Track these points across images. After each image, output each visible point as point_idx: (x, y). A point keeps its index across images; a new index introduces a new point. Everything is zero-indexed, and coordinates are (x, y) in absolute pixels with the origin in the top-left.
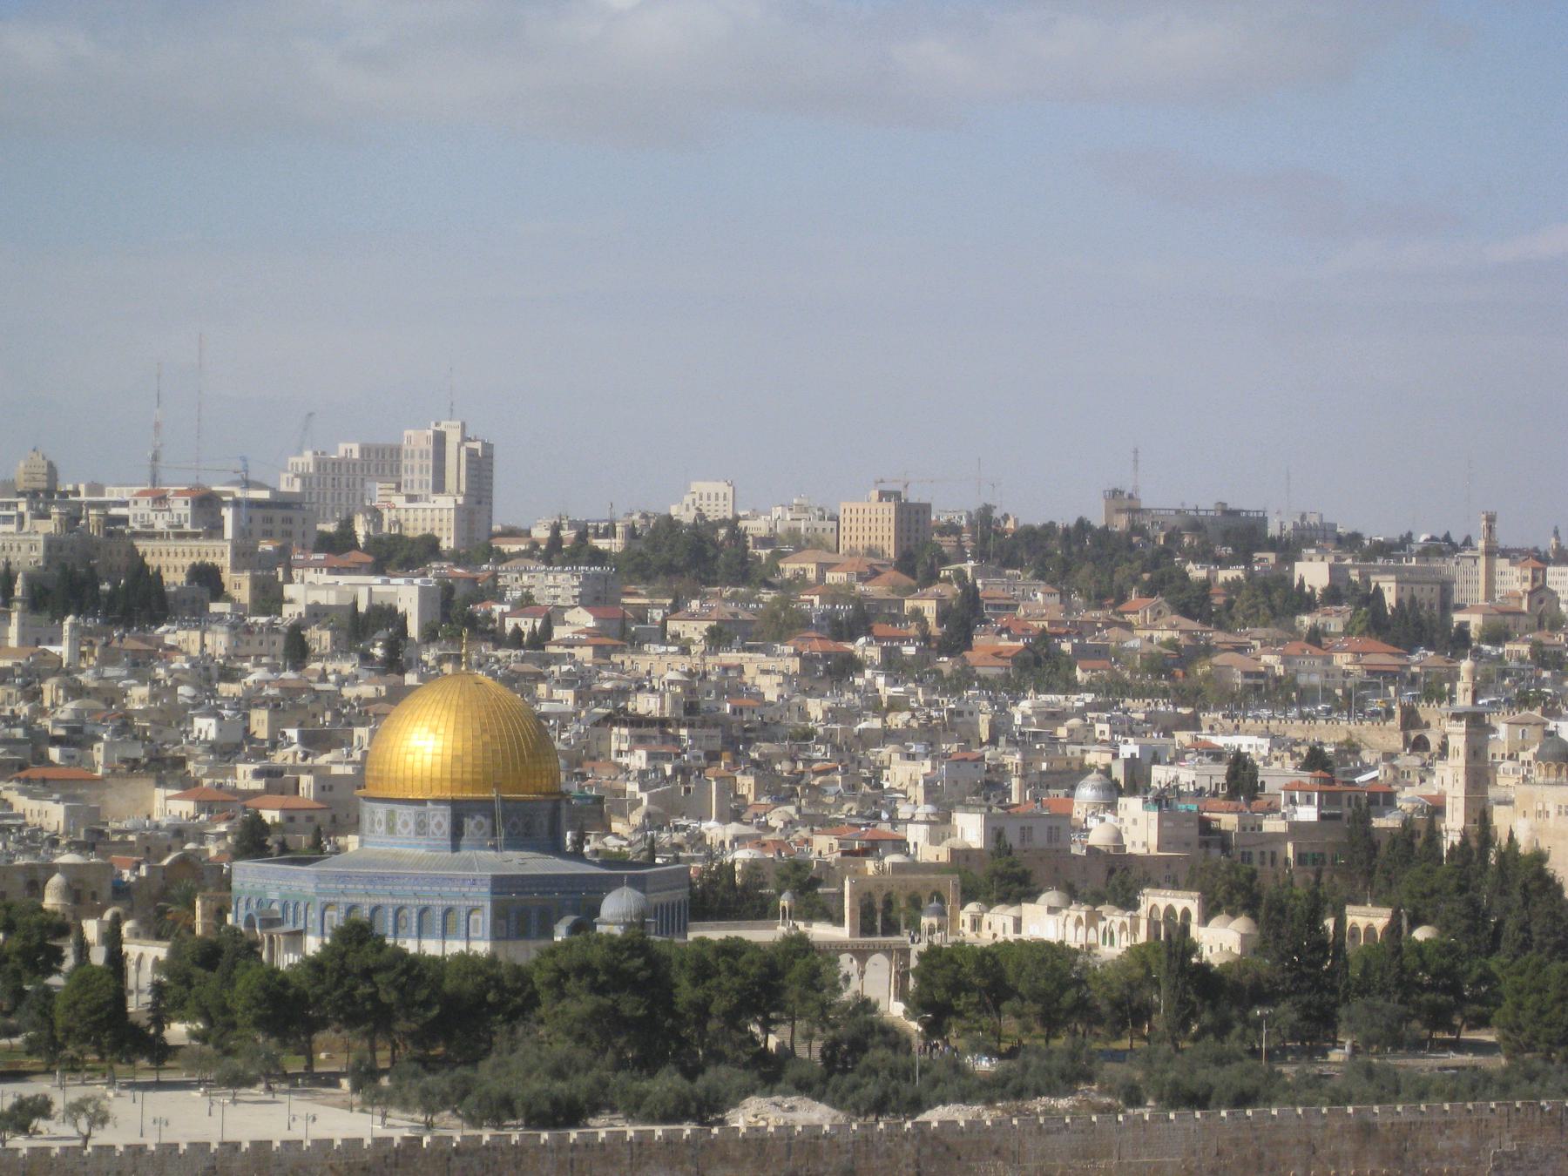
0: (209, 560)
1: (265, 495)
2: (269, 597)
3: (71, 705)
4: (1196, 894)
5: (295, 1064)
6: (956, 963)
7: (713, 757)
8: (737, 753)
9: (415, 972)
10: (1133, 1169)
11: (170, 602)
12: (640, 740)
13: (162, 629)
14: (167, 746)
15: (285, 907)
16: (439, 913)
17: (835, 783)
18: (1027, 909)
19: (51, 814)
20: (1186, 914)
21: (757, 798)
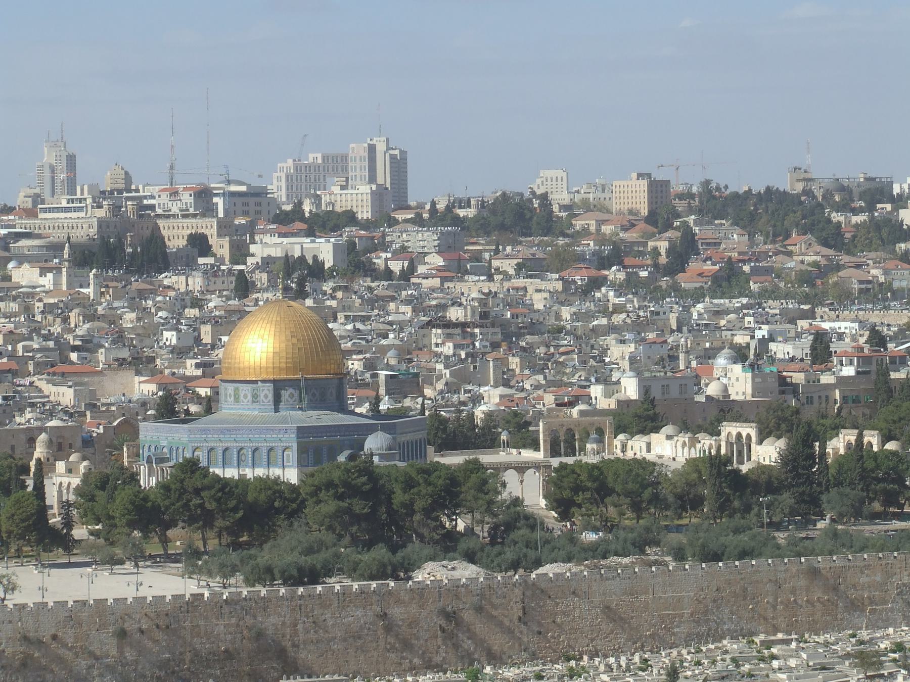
0: (200, 231)
1: (243, 188)
2: (240, 253)
3: (87, 326)
4: (754, 425)
5: (154, 548)
6: (576, 473)
7: (495, 346)
8: (511, 342)
9: (227, 490)
10: (662, 601)
11: (171, 260)
12: (449, 337)
13: (163, 275)
14: (145, 349)
15: (171, 449)
16: (265, 451)
17: (573, 359)
18: (654, 436)
19: (65, 395)
20: (749, 437)
21: (521, 370)
